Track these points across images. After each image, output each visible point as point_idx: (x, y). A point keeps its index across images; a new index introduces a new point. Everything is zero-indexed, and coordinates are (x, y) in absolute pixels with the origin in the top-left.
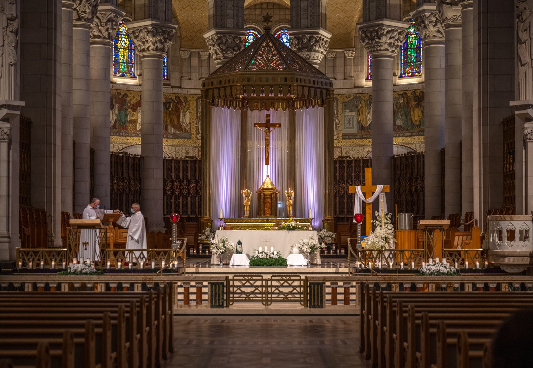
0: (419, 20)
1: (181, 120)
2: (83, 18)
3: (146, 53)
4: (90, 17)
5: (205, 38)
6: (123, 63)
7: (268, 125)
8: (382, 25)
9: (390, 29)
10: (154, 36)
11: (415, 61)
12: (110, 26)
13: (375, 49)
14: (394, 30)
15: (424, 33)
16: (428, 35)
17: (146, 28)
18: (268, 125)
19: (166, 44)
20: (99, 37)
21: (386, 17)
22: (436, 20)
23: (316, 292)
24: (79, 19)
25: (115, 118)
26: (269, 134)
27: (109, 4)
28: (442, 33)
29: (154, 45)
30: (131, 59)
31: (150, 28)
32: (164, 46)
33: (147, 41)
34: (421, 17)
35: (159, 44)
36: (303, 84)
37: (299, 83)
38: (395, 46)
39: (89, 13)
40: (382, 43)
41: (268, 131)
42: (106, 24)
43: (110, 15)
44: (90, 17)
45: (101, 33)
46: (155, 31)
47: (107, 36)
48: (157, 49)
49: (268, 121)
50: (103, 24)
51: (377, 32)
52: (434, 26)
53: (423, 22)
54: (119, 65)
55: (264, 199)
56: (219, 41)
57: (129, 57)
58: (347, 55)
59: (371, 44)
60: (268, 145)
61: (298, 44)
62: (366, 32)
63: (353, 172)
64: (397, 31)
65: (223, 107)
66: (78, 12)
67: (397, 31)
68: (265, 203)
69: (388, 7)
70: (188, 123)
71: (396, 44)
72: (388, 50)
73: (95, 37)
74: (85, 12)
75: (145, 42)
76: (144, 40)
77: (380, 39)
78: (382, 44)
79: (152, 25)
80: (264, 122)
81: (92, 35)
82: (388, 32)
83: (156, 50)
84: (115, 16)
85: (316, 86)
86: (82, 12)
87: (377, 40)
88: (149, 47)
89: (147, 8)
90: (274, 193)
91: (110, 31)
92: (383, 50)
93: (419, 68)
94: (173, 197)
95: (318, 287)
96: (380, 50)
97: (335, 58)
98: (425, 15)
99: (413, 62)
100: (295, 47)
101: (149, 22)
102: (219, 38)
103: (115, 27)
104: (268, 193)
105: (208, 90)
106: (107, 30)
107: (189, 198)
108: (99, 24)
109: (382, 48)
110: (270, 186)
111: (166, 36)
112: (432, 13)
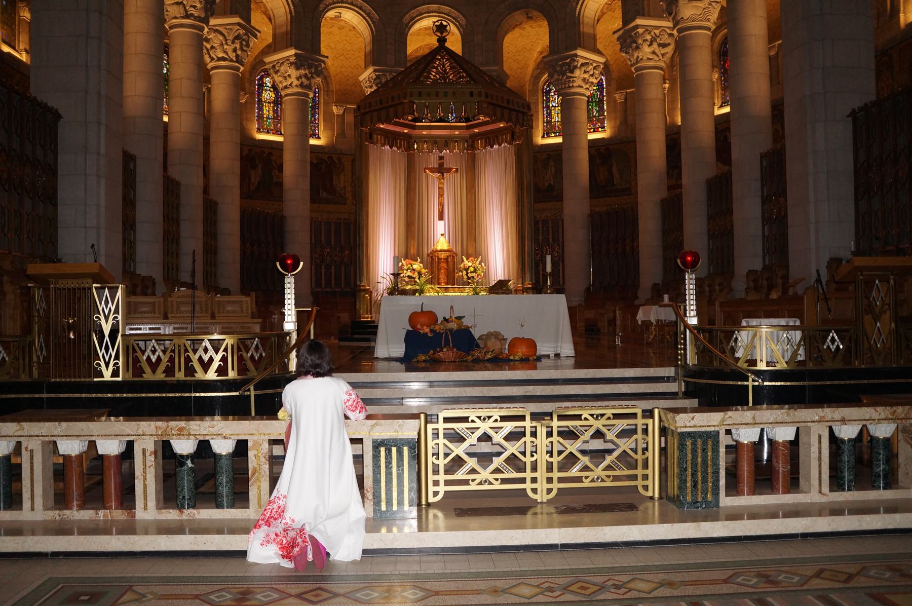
0: (628, 41)
1: (334, 183)
2: (192, 15)
3: (289, 91)
4: (203, 15)
5: (361, 80)
6: (268, 118)
8: (576, 55)
9: (584, 61)
10: (297, 69)
11: (597, 115)
12: (238, 46)
13: (567, 86)
15: (635, 57)
16: (641, 57)
17: (288, 60)
18: (442, 170)
19: (313, 81)
20: (223, 59)
21: (580, 47)
22: (651, 39)
23: (699, 460)
24: (187, 16)
25: (258, 180)
27: (236, 15)
28: (658, 56)
29: (298, 80)
30: (277, 114)
31: (293, 59)
32: (310, 83)
33: (289, 76)
34: (631, 36)
35: (304, 80)
37: (489, 100)
39: (201, 9)
40: (576, 77)
42: (233, 42)
43: (239, 31)
44: (203, 15)
45: (227, 54)
46: (299, 63)
47: (234, 59)
48: (302, 85)
49: (441, 165)
50: (229, 42)
51: (569, 64)
52: (649, 46)
53: (635, 42)
54: (263, 121)
55: (439, 263)
56: (378, 81)
57: (275, 112)
59: (561, 80)
60: (441, 195)
62: (554, 66)
63: (541, 234)
64: (592, 64)
65: (383, 145)
66: (184, 6)
67: (592, 64)
68: (439, 269)
69: (582, 36)
70: (342, 186)
71: (590, 80)
72: (582, 87)
73: (219, 59)
74: (194, 7)
75: (288, 78)
76: (286, 75)
77: (572, 72)
78: (574, 79)
79: (296, 55)
80: (436, 166)
81: (215, 57)
82: (582, 65)
83: (301, 87)
84: (246, 34)
85: (511, 106)
86: (191, 6)
87: (569, 74)
88: (292, 82)
89: (289, 36)
90: (450, 256)
91: (239, 52)
92: (577, 87)
93: (603, 123)
94: (323, 267)
95: (705, 443)
96: (573, 86)
98: (638, 32)
99: (595, 117)
101: (292, 52)
102: (378, 77)
103: (245, 48)
104: (443, 255)
105: (364, 114)
106: (235, 50)
107: (343, 267)
108: (224, 43)
109: (575, 84)
110: (446, 248)
111: (313, 70)
112: (647, 30)
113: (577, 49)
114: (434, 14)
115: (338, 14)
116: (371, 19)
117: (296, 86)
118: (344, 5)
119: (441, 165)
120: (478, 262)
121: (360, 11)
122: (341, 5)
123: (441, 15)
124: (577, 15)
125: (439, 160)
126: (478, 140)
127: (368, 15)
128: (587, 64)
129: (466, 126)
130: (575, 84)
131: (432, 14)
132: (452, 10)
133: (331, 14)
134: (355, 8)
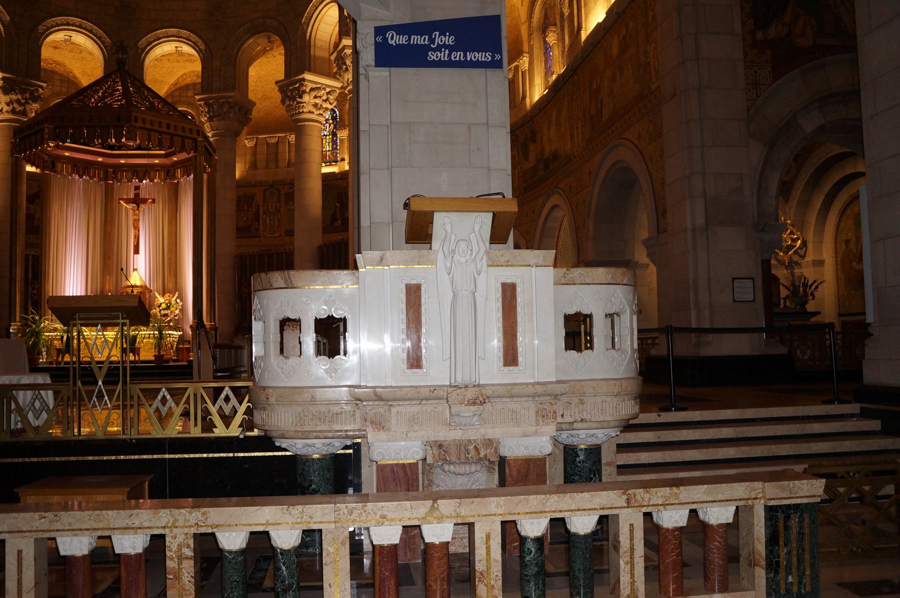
7: (138, 201)
8: (304, 80)
9: (314, 86)
13: (297, 112)
14: (320, 88)
15: (346, 79)
19: (28, 107)
26: (137, 212)
29: (8, 104)
34: (342, 57)
35: (15, 105)
36: (148, 126)
38: (323, 108)
40: (305, 102)
41: (136, 208)
58: (290, 140)
60: (137, 228)
61: (208, 112)
62: (286, 91)
67: (324, 89)
72: (313, 113)
77: (301, 97)
80: (132, 196)
82: (312, 89)
87: (299, 100)
92: (307, 112)
97: (277, 143)
98: (345, 53)
100: (205, 116)
111: (28, 95)
113: (304, 73)
114: (173, 38)
115: (67, 37)
116: (103, 43)
117: (7, 112)
118: (71, 27)
119: (137, 195)
120: (174, 299)
121: (91, 35)
122: (66, 27)
123: (180, 39)
124: (308, 38)
125: (135, 190)
126: (177, 169)
127: (100, 38)
128: (319, 88)
129: (166, 154)
130: (305, 110)
131: (171, 39)
132: (192, 34)
133: (59, 36)
134: (84, 31)
